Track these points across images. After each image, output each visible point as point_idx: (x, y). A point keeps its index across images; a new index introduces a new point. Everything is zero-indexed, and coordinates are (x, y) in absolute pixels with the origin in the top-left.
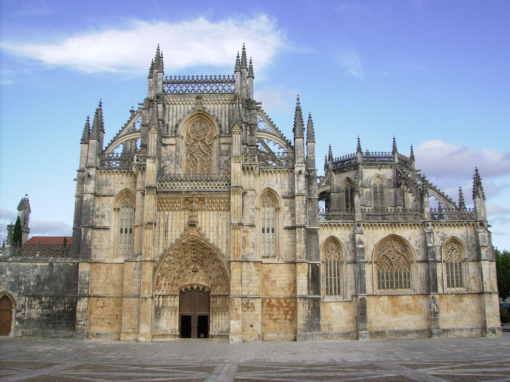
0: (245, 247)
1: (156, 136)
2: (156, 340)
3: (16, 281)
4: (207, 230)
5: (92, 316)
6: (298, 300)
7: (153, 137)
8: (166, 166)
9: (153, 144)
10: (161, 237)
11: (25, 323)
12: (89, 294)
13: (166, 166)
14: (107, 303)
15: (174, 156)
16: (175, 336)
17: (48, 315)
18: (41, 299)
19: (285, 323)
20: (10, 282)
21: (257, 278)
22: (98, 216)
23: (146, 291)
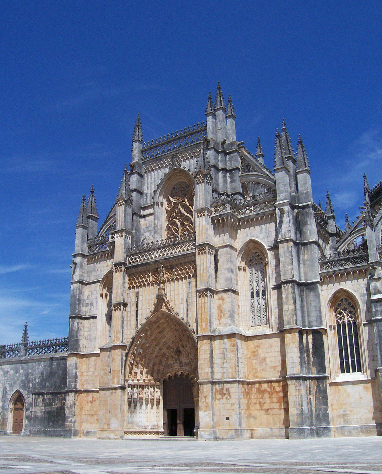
0: (221, 318)
1: (123, 206)
2: (129, 436)
3: (26, 380)
4: (177, 302)
5: (84, 413)
6: (289, 382)
7: (121, 209)
8: (146, 238)
9: (121, 217)
10: (134, 318)
11: (32, 421)
12: (79, 387)
13: (146, 238)
14: (95, 397)
15: (153, 226)
16: (157, 433)
17: (49, 413)
18: (44, 397)
19: (280, 414)
20: (22, 381)
21: (232, 355)
22: (87, 305)
23: (116, 381)
